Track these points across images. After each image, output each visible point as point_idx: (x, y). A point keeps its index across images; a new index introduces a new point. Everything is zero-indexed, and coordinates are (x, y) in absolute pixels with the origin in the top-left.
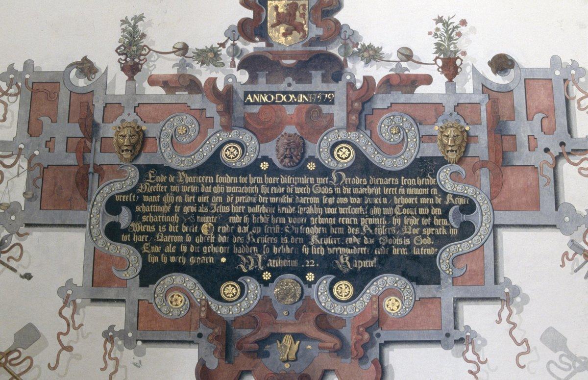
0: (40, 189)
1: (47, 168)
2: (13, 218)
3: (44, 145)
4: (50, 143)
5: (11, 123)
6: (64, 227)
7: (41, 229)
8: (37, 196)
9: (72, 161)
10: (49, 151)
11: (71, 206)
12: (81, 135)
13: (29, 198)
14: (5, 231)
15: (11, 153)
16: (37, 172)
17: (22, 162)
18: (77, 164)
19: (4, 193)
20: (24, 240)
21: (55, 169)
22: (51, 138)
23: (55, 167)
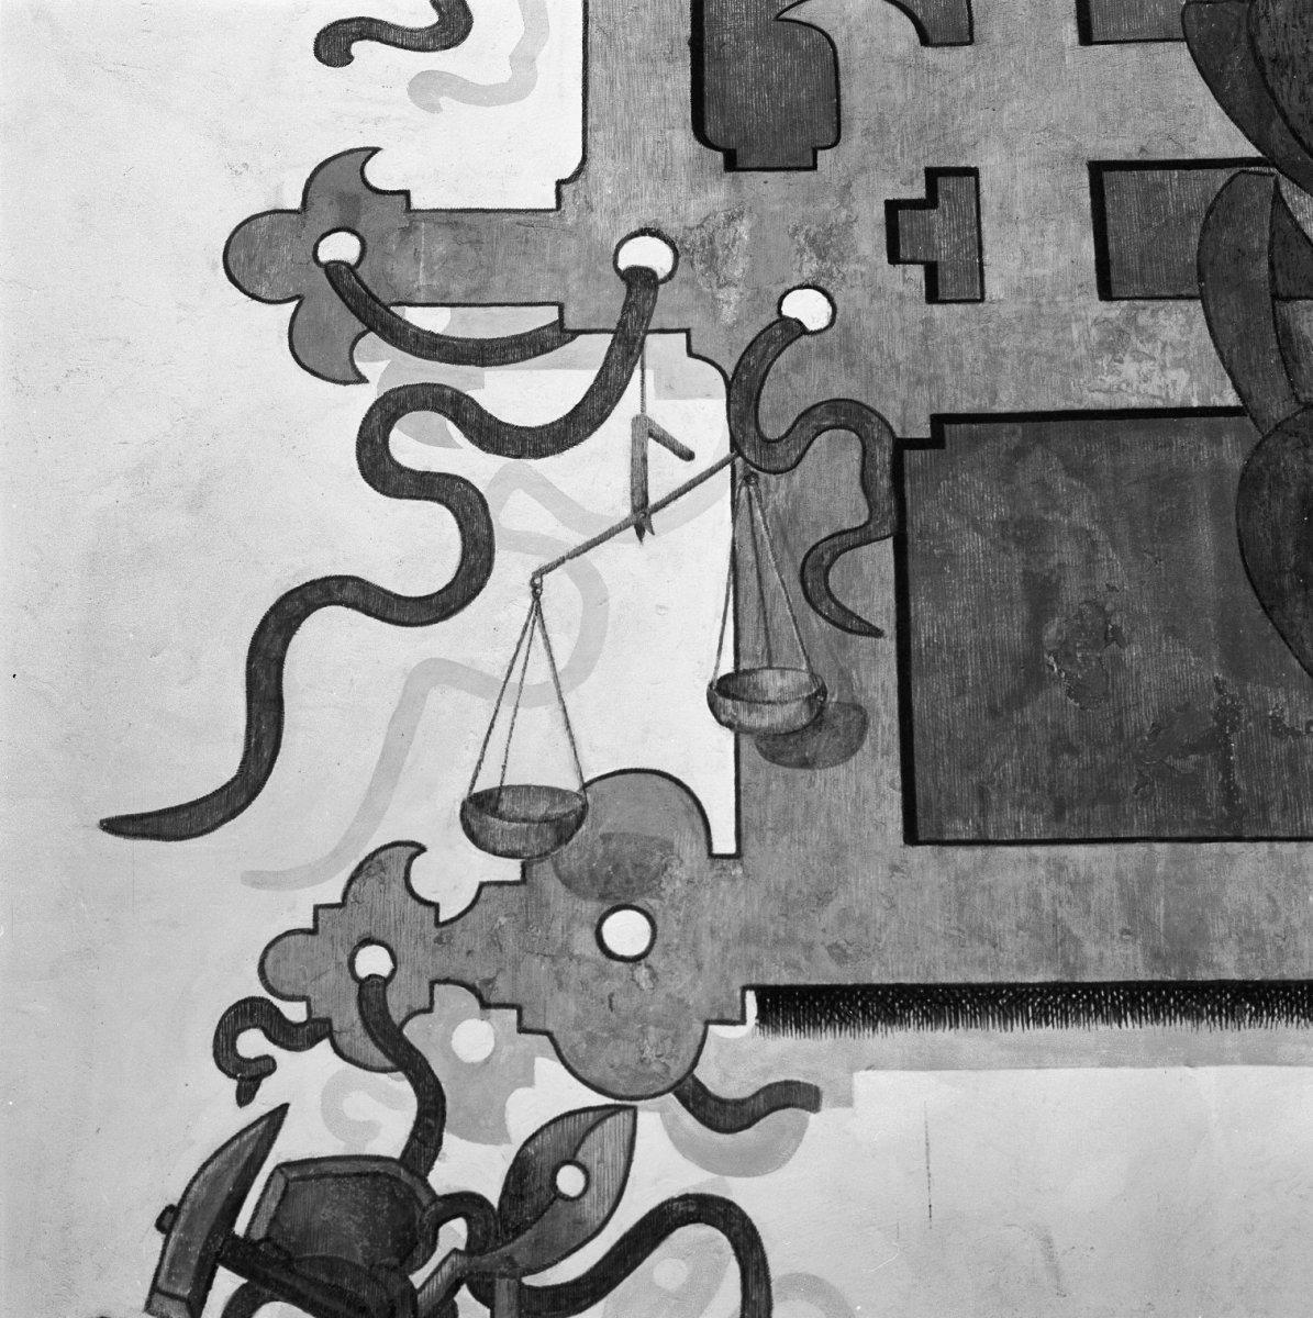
0: (889, 645)
1: (936, 442)
2: (627, 932)
3: (870, 239)
4: (934, 226)
5: (524, 60)
6: (1196, 1015)
7: (944, 1037)
8: (861, 718)
9: (1180, 376)
10: (933, 296)
11: (1230, 793)
12: (1221, 137)
13: (785, 738)
14: (549, 1069)
15: (551, 314)
16: (831, 482)
17: (669, 389)
18: (1231, 399)
19: (506, 690)
20: (755, 1164)
21: (1019, 453)
22: (933, 175)
23: (1012, 435)
